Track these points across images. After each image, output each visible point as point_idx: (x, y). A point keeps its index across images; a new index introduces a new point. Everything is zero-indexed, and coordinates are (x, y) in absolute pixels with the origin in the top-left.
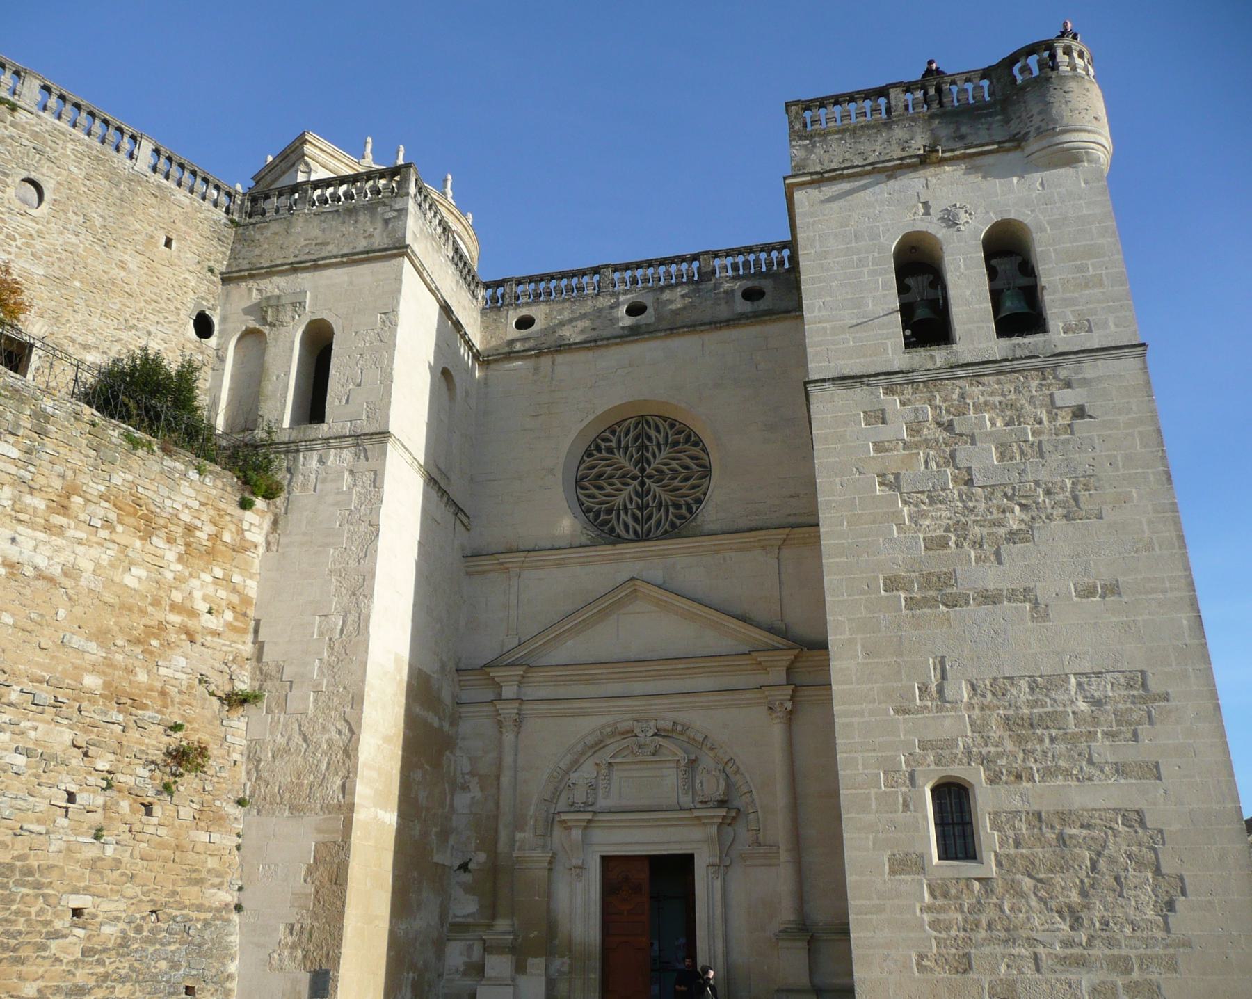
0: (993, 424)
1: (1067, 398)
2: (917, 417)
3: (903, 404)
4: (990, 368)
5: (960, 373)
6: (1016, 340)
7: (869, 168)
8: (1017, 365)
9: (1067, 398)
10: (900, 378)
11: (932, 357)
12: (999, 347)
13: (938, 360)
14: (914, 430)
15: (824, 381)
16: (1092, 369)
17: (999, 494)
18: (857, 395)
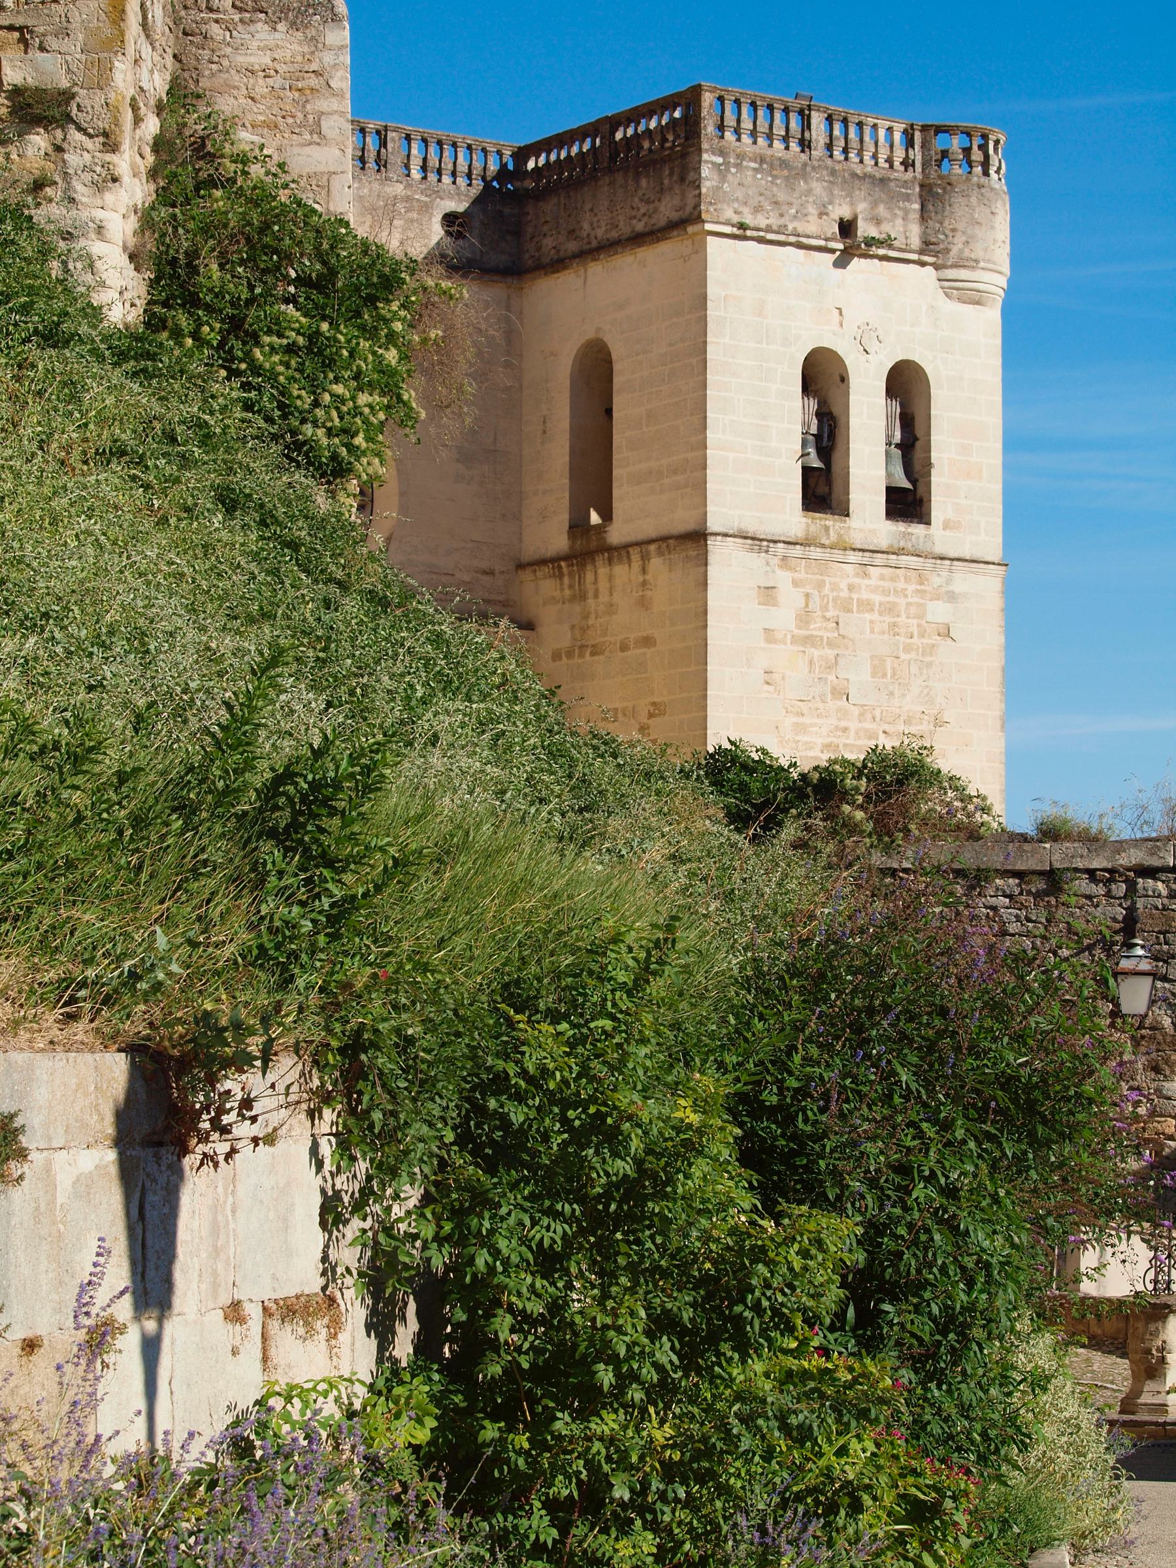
0: (872, 631)
1: (938, 612)
2: (807, 605)
3: (795, 584)
4: (879, 559)
5: (853, 557)
6: (901, 527)
7: (792, 239)
8: (905, 560)
9: (938, 612)
10: (798, 551)
11: (827, 529)
12: (886, 531)
13: (831, 532)
14: (804, 618)
15: (726, 535)
16: (964, 581)
17: (869, 716)
18: (756, 561)
